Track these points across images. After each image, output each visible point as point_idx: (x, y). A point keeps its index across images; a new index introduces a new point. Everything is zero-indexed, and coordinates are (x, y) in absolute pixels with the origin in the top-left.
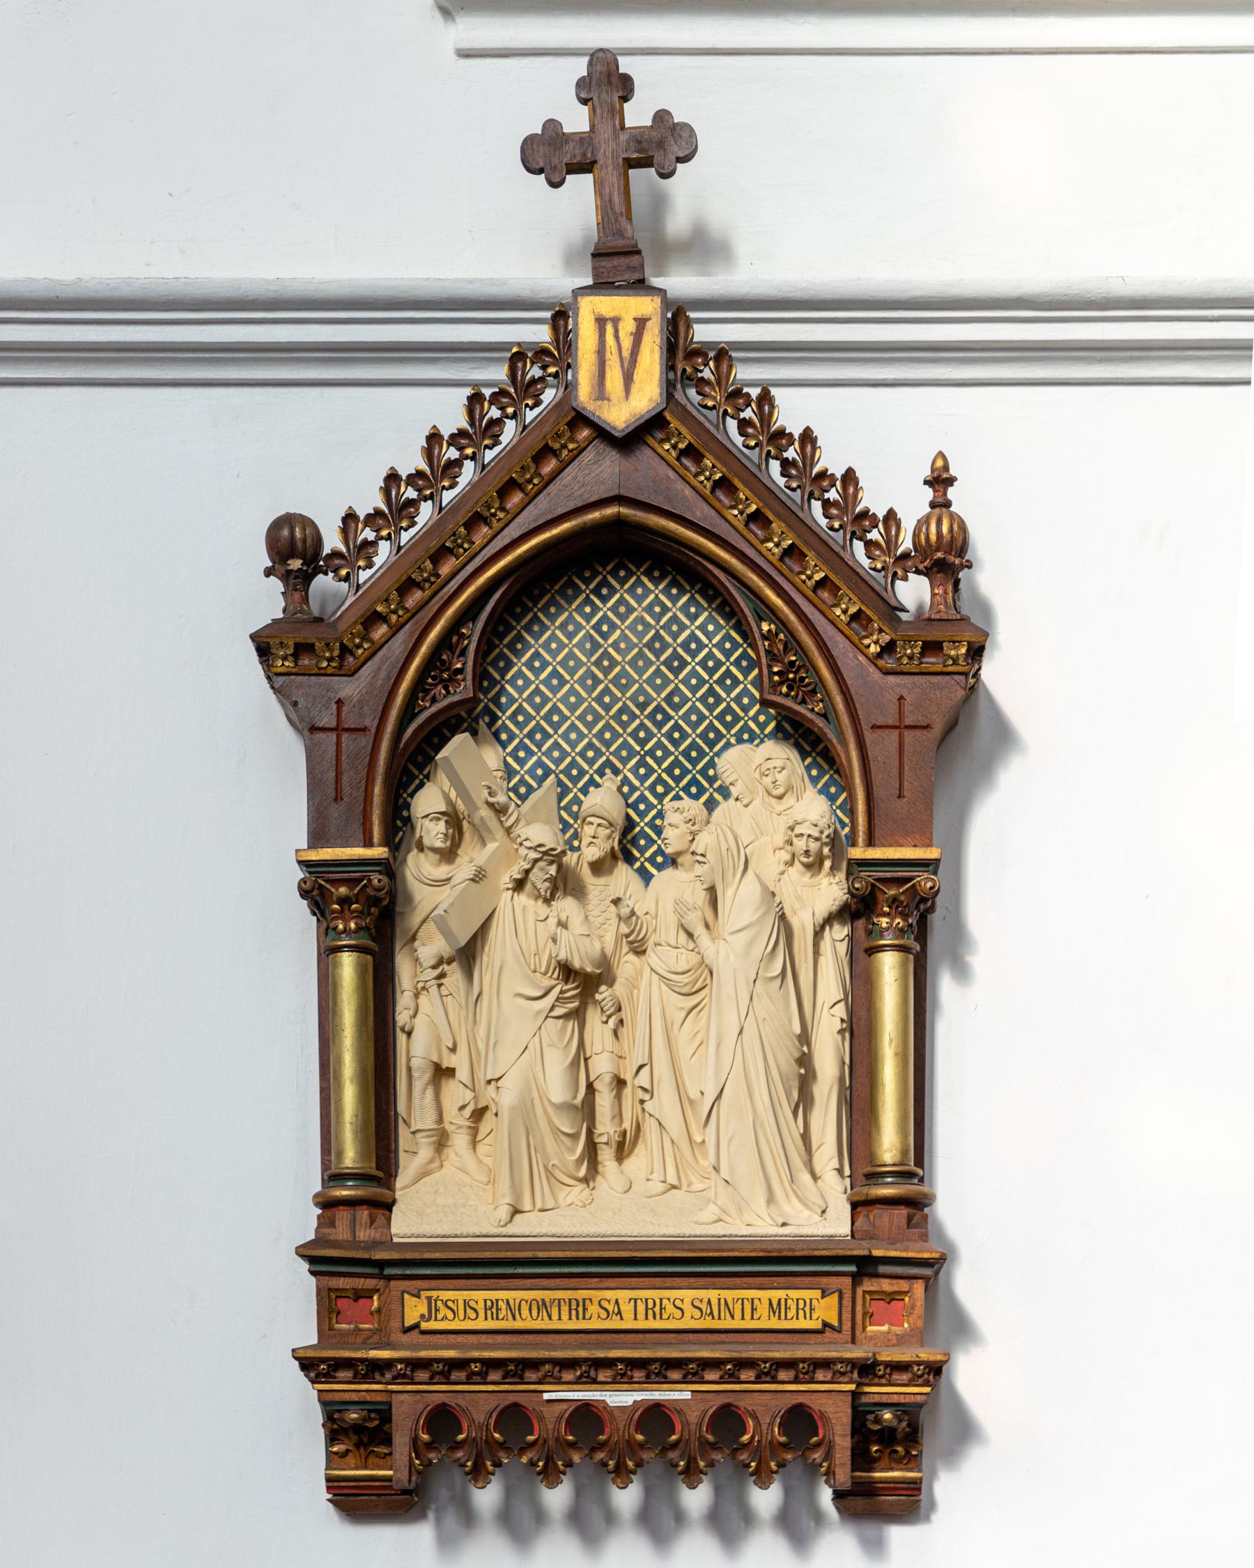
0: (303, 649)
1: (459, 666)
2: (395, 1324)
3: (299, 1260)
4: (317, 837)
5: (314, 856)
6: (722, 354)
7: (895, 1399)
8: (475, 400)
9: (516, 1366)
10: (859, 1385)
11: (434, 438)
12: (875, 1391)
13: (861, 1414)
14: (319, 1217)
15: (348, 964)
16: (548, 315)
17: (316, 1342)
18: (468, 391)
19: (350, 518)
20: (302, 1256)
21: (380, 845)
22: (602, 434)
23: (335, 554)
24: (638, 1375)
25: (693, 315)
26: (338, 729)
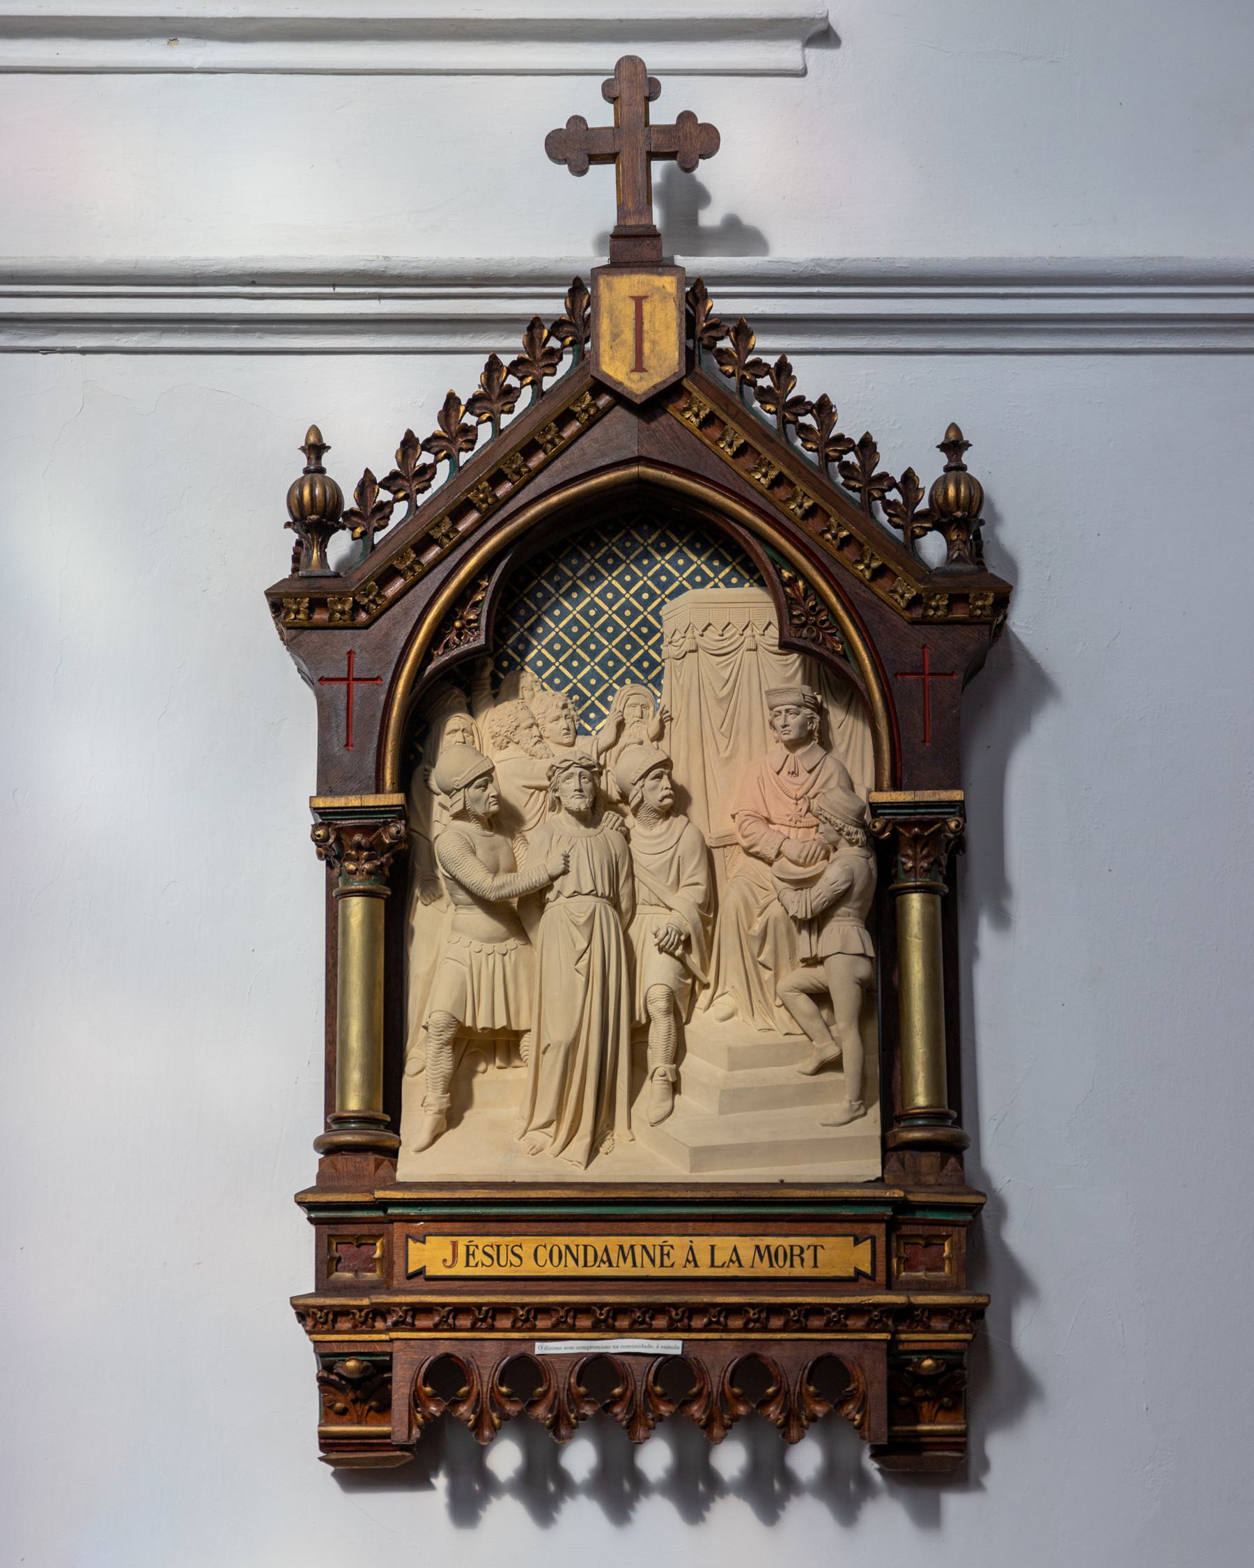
0: (317, 603)
1: (472, 617)
2: (398, 1269)
3: (298, 1207)
4: (326, 785)
5: (321, 803)
6: (742, 328)
7: (934, 1346)
8: (493, 366)
9: (644, 1313)
10: (894, 1334)
11: (452, 400)
12: (912, 1338)
13: (897, 1360)
14: (321, 1161)
15: (356, 908)
16: (565, 290)
17: (313, 1291)
18: (485, 359)
19: (368, 477)
20: (300, 1203)
21: (393, 791)
22: (621, 399)
23: (352, 512)
24: (585, 1322)
25: (711, 290)
26: (348, 679)
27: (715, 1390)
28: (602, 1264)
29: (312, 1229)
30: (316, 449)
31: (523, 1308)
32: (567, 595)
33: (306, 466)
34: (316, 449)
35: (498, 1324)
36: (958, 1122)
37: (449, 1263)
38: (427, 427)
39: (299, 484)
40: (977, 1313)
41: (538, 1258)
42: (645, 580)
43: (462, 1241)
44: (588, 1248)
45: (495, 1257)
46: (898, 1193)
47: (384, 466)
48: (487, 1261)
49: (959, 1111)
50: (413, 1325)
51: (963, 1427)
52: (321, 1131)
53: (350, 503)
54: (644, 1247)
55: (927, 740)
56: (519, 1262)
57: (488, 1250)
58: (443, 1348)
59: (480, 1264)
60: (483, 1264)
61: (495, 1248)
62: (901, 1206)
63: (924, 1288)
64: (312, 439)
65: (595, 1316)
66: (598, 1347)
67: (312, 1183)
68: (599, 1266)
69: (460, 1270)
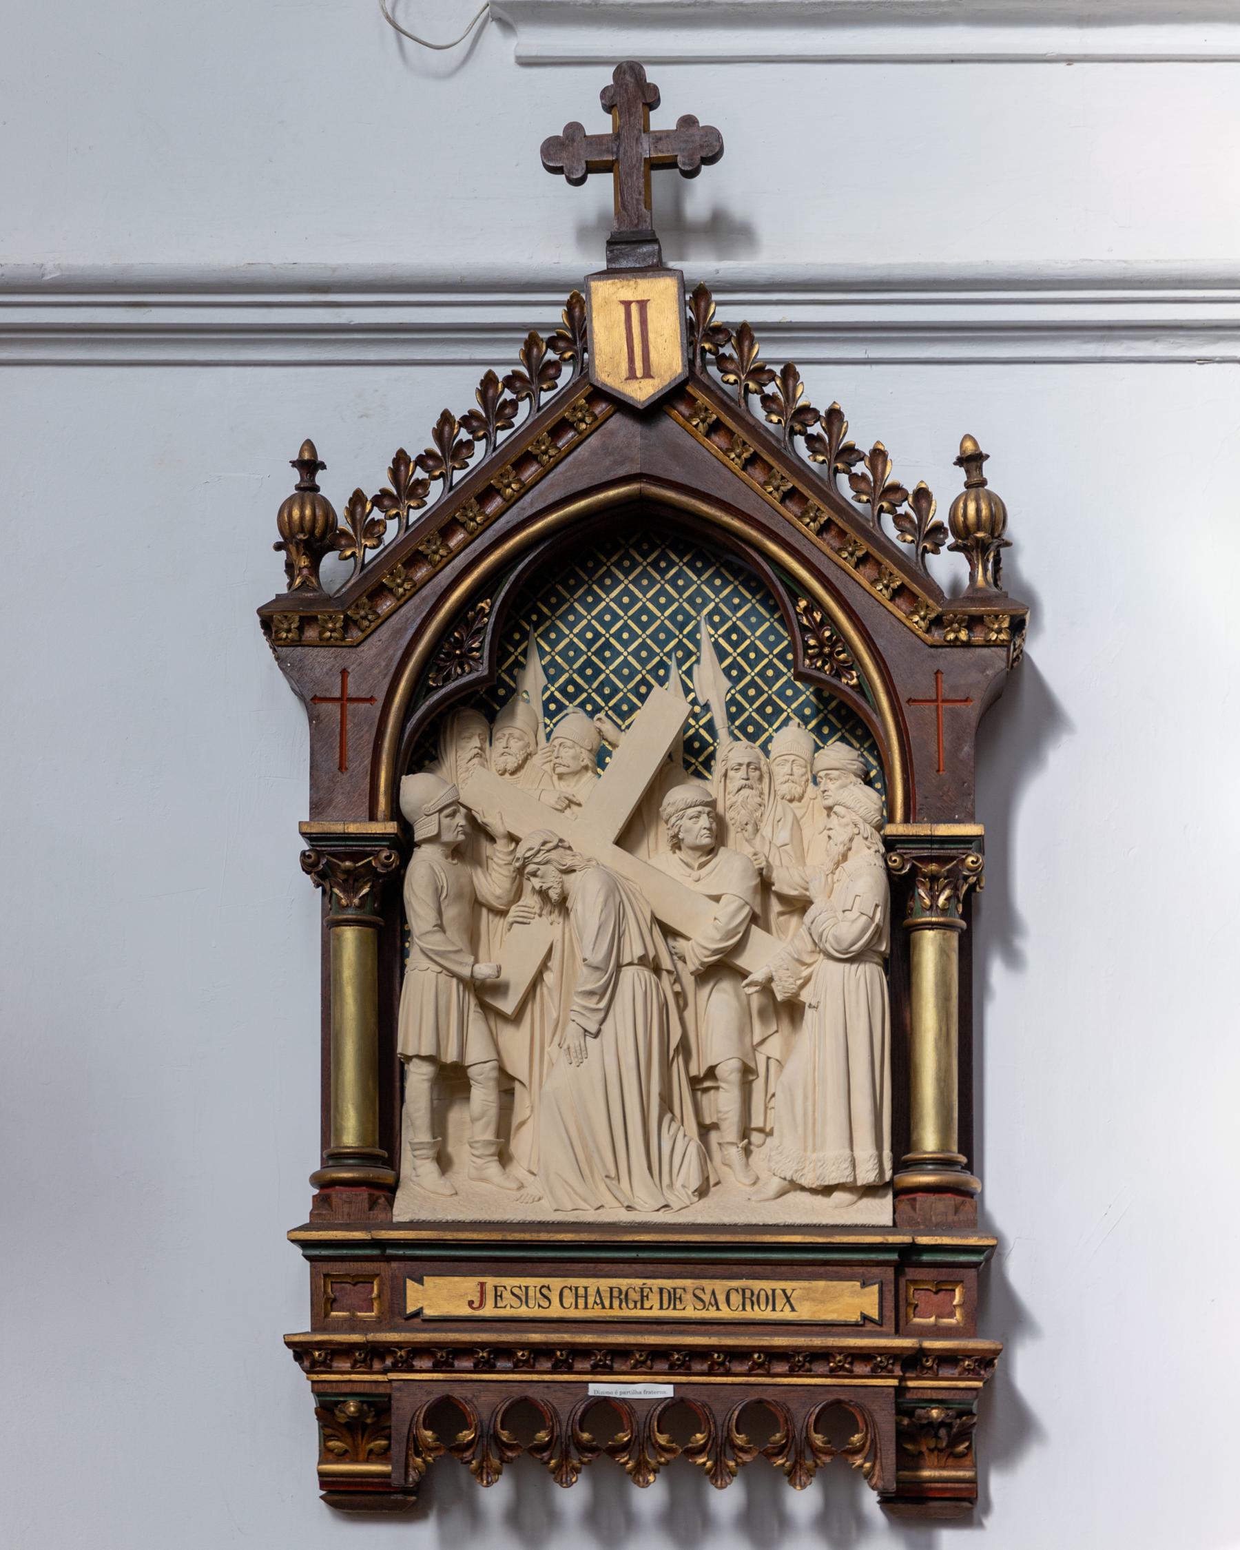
27: (564, 1434)
28: (710, 1307)
29: (308, 1263)
30: (309, 465)
31: (678, 1352)
32: (563, 618)
33: (298, 482)
34: (309, 465)
35: (538, 1367)
36: (969, 1167)
37: (476, 1304)
38: (421, 442)
39: (289, 503)
40: (985, 1361)
41: (564, 1300)
42: (607, 600)
43: (490, 1282)
44: (746, 1291)
45: (524, 1300)
46: (907, 1239)
47: (378, 480)
48: (516, 1302)
49: (970, 1157)
50: (611, 1367)
51: (900, 1473)
52: (317, 1167)
53: (343, 523)
54: (784, 1291)
55: (941, 769)
56: (548, 1303)
57: (516, 1291)
58: (445, 1390)
59: (509, 1306)
60: (511, 1307)
61: (523, 1289)
62: (909, 1253)
63: (938, 1332)
64: (307, 456)
65: (436, 1357)
66: (636, 1392)
67: (306, 1220)
68: (707, 1310)
69: (488, 1311)
